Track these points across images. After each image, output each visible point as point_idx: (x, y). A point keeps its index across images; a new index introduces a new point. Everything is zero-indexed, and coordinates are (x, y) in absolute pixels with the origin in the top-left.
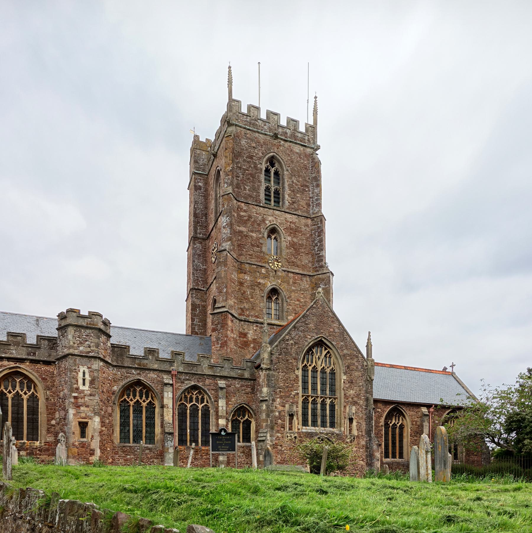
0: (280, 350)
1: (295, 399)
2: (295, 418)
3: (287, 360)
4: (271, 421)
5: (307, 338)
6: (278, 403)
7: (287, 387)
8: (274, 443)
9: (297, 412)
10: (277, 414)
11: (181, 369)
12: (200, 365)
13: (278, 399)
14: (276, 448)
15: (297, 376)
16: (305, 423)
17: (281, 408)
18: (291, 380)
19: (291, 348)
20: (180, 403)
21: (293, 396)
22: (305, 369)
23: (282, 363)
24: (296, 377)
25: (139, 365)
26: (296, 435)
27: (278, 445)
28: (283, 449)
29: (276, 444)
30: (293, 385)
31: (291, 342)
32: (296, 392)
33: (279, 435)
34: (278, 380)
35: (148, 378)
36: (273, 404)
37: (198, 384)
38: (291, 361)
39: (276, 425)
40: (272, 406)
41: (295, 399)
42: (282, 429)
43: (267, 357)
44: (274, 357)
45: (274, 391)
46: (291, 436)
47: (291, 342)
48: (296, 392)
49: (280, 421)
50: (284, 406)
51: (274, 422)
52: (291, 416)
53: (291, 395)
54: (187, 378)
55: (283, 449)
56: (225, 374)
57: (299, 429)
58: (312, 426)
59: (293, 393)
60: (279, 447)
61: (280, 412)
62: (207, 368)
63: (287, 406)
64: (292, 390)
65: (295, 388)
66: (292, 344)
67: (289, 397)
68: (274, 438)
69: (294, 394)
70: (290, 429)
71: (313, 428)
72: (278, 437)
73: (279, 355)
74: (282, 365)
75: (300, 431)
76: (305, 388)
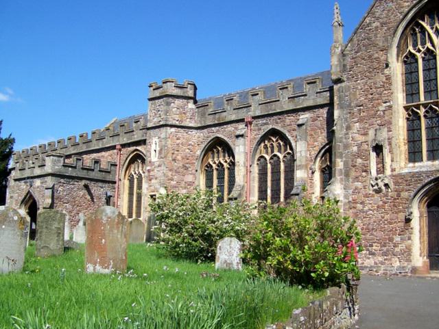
0: (358, 44)
1: (386, 118)
2: (386, 151)
3: (370, 57)
4: (346, 164)
5: (403, 7)
6: (355, 131)
7: (372, 100)
8: (351, 199)
9: (389, 139)
10: (355, 149)
11: (258, 113)
12: (278, 101)
13: (357, 124)
14: (354, 208)
15: (388, 78)
16: (414, 155)
17: (362, 138)
18: (376, 88)
19: (376, 36)
20: (257, 157)
21: (382, 113)
22: (410, 60)
23: (361, 64)
24: (387, 79)
25: (219, 119)
26: (386, 181)
27: (356, 203)
28: (366, 208)
29: (355, 201)
30: (381, 94)
31: (374, 25)
32: (388, 104)
33: (359, 185)
34: (355, 94)
35: (223, 133)
36: (347, 134)
37: (276, 128)
38: (376, 55)
39: (354, 169)
40: (346, 138)
41: (386, 118)
42: (364, 174)
43: (336, 63)
44: (348, 59)
45: (350, 113)
46: (377, 184)
47: (374, 25)
48: (388, 104)
49: (359, 161)
50: (366, 134)
51: (350, 163)
52: (378, 149)
53: (379, 112)
54: (264, 121)
55: (366, 208)
56: (310, 103)
57: (393, 170)
58: (429, 159)
59: (381, 108)
60: (359, 206)
61: (359, 146)
62: (286, 102)
63: (371, 132)
64: (379, 104)
65: (384, 99)
66: (377, 27)
67: (374, 116)
68: (351, 191)
69: (384, 109)
70: (381, 170)
71: (430, 163)
72: (356, 189)
73: (357, 52)
74: (363, 67)
75: (394, 173)
76: (411, 93)
